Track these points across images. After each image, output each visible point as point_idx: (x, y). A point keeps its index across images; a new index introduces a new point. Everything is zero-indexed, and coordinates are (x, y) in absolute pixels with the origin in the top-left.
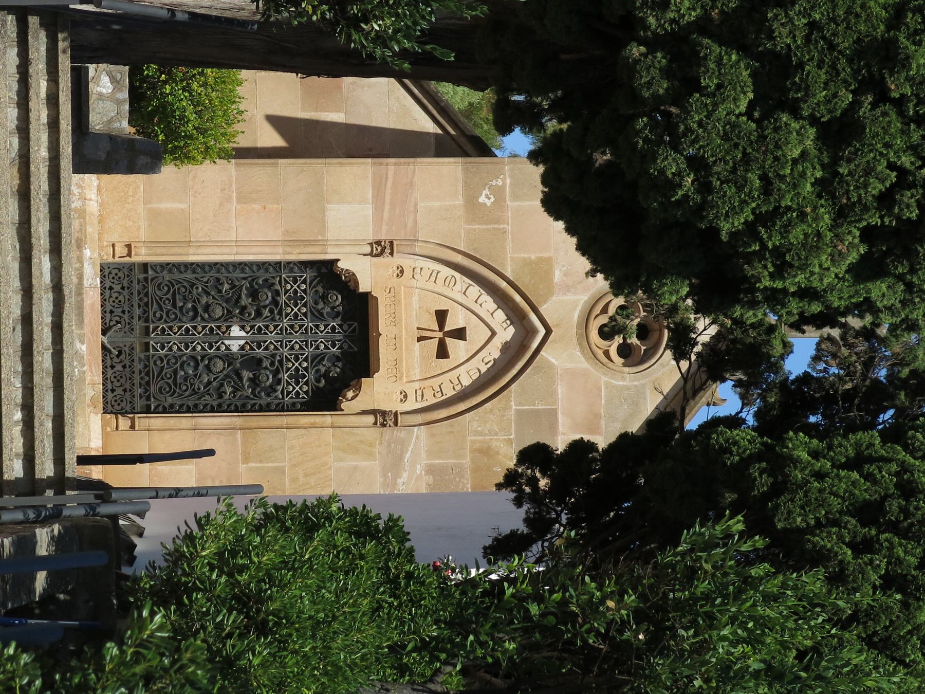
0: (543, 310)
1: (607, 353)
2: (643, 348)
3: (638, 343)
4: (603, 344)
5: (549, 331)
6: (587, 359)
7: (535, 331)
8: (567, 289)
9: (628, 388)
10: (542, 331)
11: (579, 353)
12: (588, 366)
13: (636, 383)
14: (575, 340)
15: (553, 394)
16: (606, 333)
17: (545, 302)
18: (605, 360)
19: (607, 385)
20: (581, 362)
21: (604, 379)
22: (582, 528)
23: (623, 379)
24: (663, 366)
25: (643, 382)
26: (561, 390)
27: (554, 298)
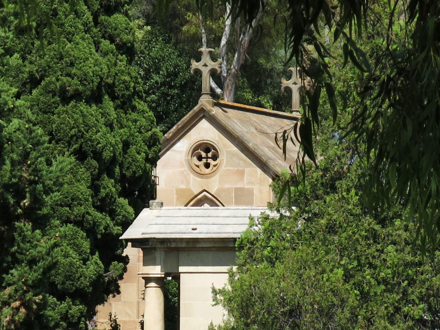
0: (196, 193)
1: (215, 166)
2: (213, 151)
3: (211, 152)
4: (211, 166)
5: (205, 190)
6: (215, 175)
7: (205, 196)
8: (188, 183)
9: (227, 158)
10: (205, 193)
11: (213, 178)
12: (219, 173)
13: (225, 154)
14: (208, 180)
15: (228, 189)
16: (207, 166)
17: (192, 192)
18: (216, 167)
19: (225, 166)
20: (216, 178)
21: (223, 167)
22: (406, 82)
23: (223, 160)
24: (219, 143)
25: (224, 151)
26: (227, 186)
27: (191, 188)
